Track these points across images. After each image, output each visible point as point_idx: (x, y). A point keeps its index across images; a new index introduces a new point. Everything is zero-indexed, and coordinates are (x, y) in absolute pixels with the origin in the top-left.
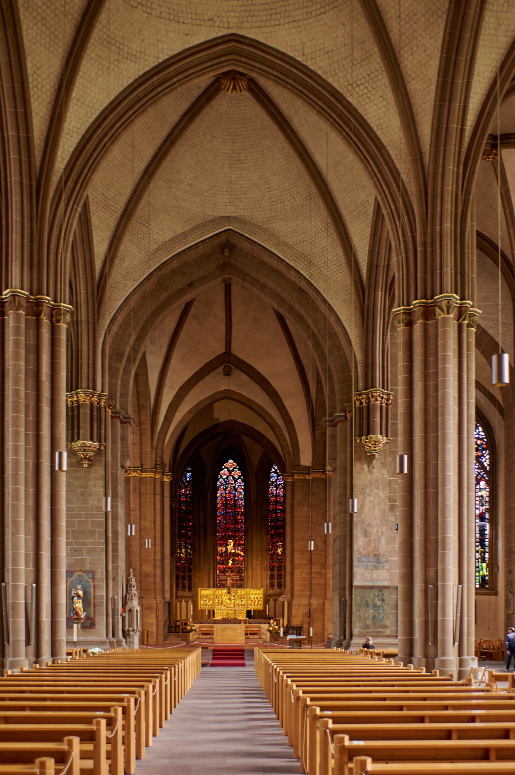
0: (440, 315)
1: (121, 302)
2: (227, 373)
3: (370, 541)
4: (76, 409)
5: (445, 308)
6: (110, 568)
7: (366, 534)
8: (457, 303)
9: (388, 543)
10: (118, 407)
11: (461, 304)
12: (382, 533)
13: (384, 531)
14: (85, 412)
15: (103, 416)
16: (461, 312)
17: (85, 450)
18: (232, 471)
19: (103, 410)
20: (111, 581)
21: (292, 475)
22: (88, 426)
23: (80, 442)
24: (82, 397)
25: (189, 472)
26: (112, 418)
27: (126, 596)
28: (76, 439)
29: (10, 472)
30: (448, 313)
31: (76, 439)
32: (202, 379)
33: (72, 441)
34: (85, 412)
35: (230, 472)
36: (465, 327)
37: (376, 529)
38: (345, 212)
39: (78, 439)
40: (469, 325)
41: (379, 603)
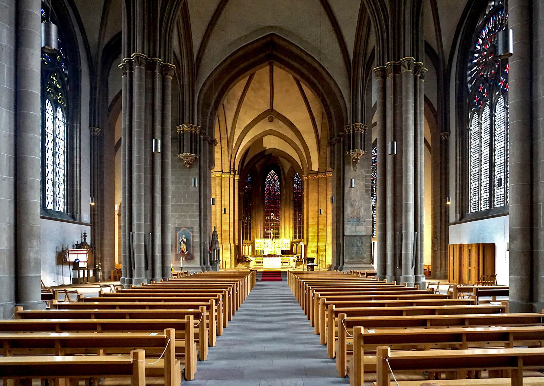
0: (404, 70)
1: (208, 75)
2: (271, 121)
3: (355, 209)
4: (182, 135)
5: (407, 66)
6: (202, 226)
7: (352, 205)
8: (414, 64)
9: (365, 211)
10: (207, 134)
11: (416, 64)
12: (362, 205)
13: (363, 203)
14: (187, 137)
15: (198, 139)
16: (416, 69)
17: (187, 158)
18: (274, 176)
19: (198, 136)
20: (202, 233)
21: (307, 176)
22: (189, 144)
23: (184, 154)
24: (186, 128)
25: (249, 177)
26: (204, 140)
27: (212, 241)
28: (182, 152)
29: (135, 164)
30: (409, 69)
31: (182, 152)
32: (256, 124)
33: (180, 153)
34: (187, 137)
35: (272, 177)
36: (418, 78)
37: (358, 203)
38: (340, 23)
39: (183, 152)
40: (421, 78)
41: (360, 245)
